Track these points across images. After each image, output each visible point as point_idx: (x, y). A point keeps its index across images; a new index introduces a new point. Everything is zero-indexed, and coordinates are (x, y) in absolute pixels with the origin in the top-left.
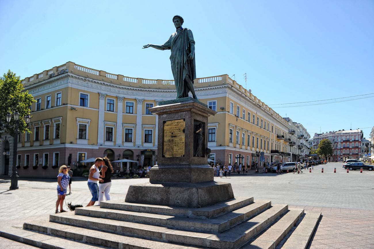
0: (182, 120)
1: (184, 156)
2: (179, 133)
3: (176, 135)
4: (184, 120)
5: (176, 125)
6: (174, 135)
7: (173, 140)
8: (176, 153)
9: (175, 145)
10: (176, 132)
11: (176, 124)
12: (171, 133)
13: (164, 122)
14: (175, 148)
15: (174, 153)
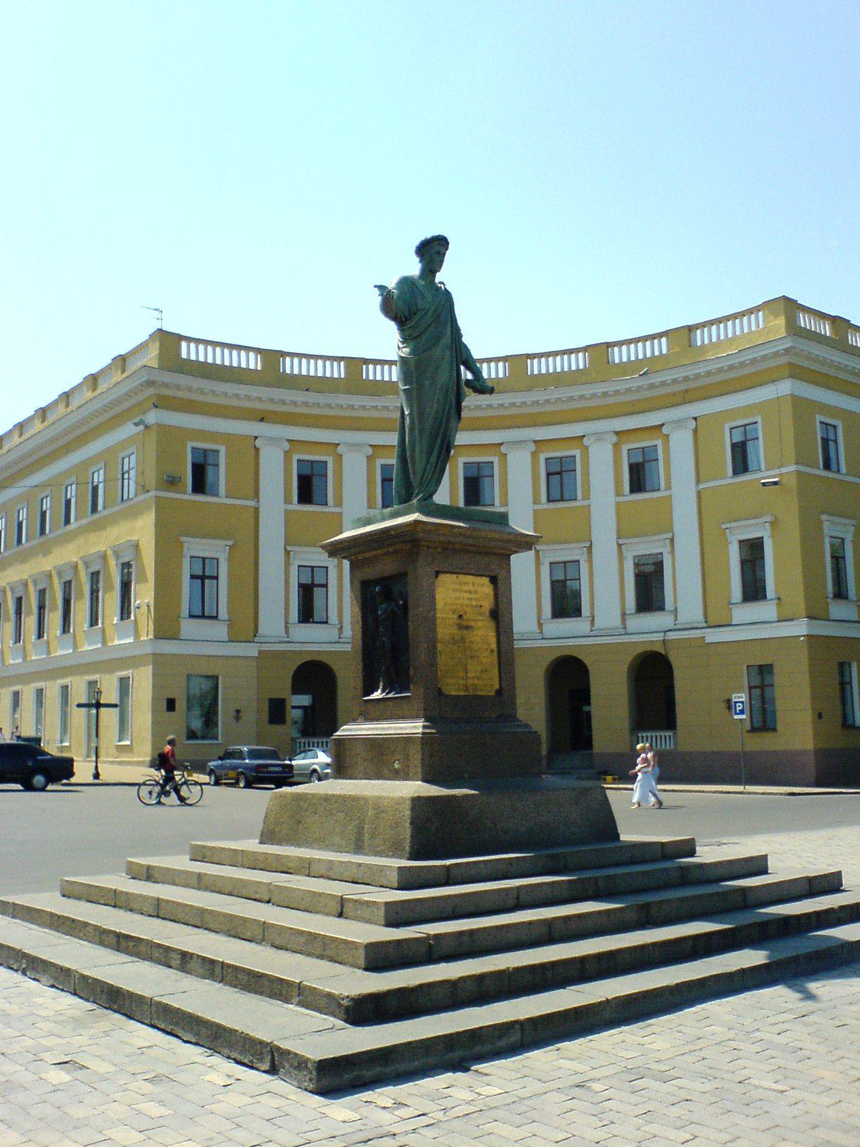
0: (486, 580)
1: (499, 692)
2: (480, 618)
3: (472, 624)
4: (494, 580)
5: (470, 592)
6: (466, 623)
7: (463, 638)
8: (476, 681)
9: (472, 658)
10: (470, 614)
11: (471, 587)
12: (456, 616)
13: (437, 574)
14: (474, 669)
15: (470, 682)
